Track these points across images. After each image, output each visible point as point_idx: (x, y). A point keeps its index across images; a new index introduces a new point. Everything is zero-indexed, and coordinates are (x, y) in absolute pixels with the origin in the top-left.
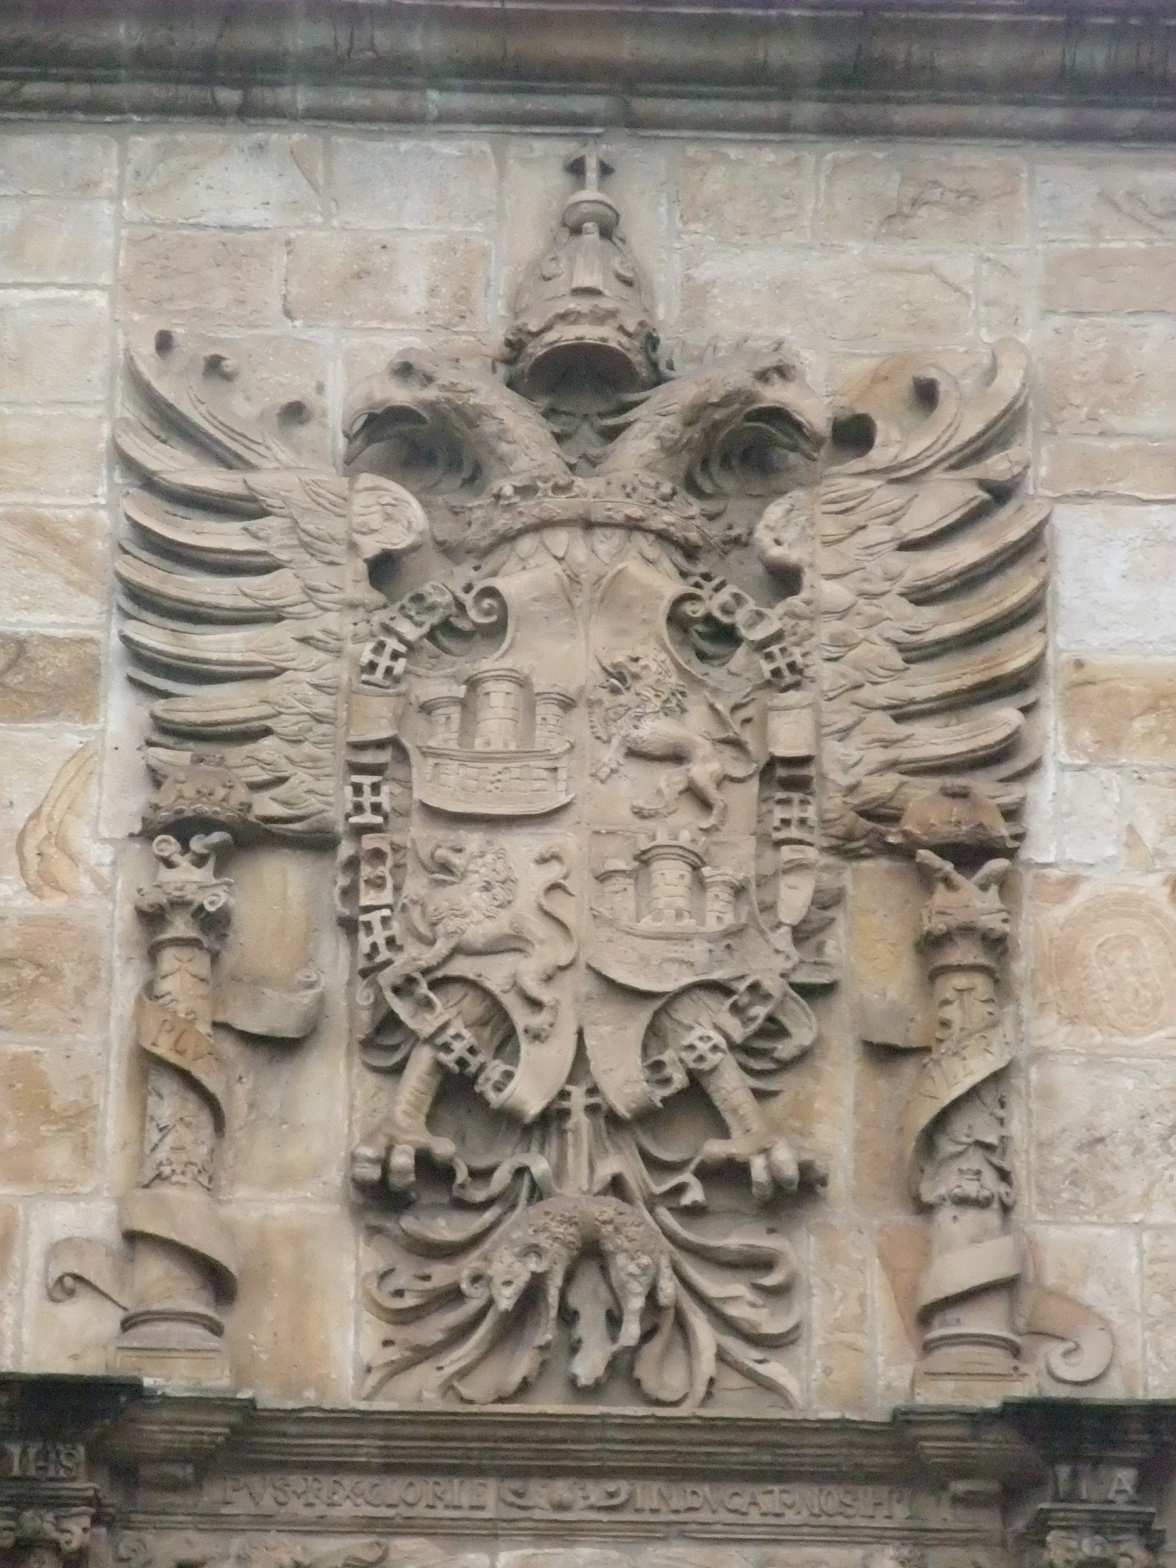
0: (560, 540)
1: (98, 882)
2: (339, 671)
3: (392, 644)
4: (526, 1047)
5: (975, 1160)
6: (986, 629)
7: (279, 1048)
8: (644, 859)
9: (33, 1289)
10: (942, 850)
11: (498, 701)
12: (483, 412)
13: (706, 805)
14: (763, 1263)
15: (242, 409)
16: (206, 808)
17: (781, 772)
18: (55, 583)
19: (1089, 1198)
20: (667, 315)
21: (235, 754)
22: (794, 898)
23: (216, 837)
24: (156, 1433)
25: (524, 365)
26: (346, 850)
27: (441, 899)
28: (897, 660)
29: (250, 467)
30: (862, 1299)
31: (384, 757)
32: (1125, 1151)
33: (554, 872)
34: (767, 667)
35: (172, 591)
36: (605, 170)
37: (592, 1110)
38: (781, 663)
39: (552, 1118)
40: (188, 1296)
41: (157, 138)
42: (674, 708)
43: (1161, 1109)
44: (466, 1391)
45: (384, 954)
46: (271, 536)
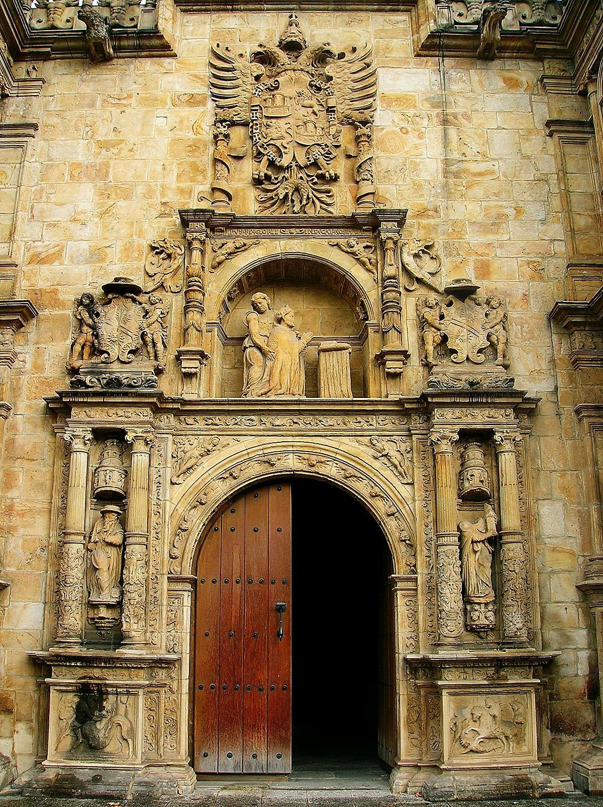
5: (367, 173)
6: (366, 87)
7: (238, 158)
11: (279, 98)
22: (333, 130)
24: (218, 221)
27: (268, 131)
33: (288, 126)
39: (289, 167)
40: (224, 197)
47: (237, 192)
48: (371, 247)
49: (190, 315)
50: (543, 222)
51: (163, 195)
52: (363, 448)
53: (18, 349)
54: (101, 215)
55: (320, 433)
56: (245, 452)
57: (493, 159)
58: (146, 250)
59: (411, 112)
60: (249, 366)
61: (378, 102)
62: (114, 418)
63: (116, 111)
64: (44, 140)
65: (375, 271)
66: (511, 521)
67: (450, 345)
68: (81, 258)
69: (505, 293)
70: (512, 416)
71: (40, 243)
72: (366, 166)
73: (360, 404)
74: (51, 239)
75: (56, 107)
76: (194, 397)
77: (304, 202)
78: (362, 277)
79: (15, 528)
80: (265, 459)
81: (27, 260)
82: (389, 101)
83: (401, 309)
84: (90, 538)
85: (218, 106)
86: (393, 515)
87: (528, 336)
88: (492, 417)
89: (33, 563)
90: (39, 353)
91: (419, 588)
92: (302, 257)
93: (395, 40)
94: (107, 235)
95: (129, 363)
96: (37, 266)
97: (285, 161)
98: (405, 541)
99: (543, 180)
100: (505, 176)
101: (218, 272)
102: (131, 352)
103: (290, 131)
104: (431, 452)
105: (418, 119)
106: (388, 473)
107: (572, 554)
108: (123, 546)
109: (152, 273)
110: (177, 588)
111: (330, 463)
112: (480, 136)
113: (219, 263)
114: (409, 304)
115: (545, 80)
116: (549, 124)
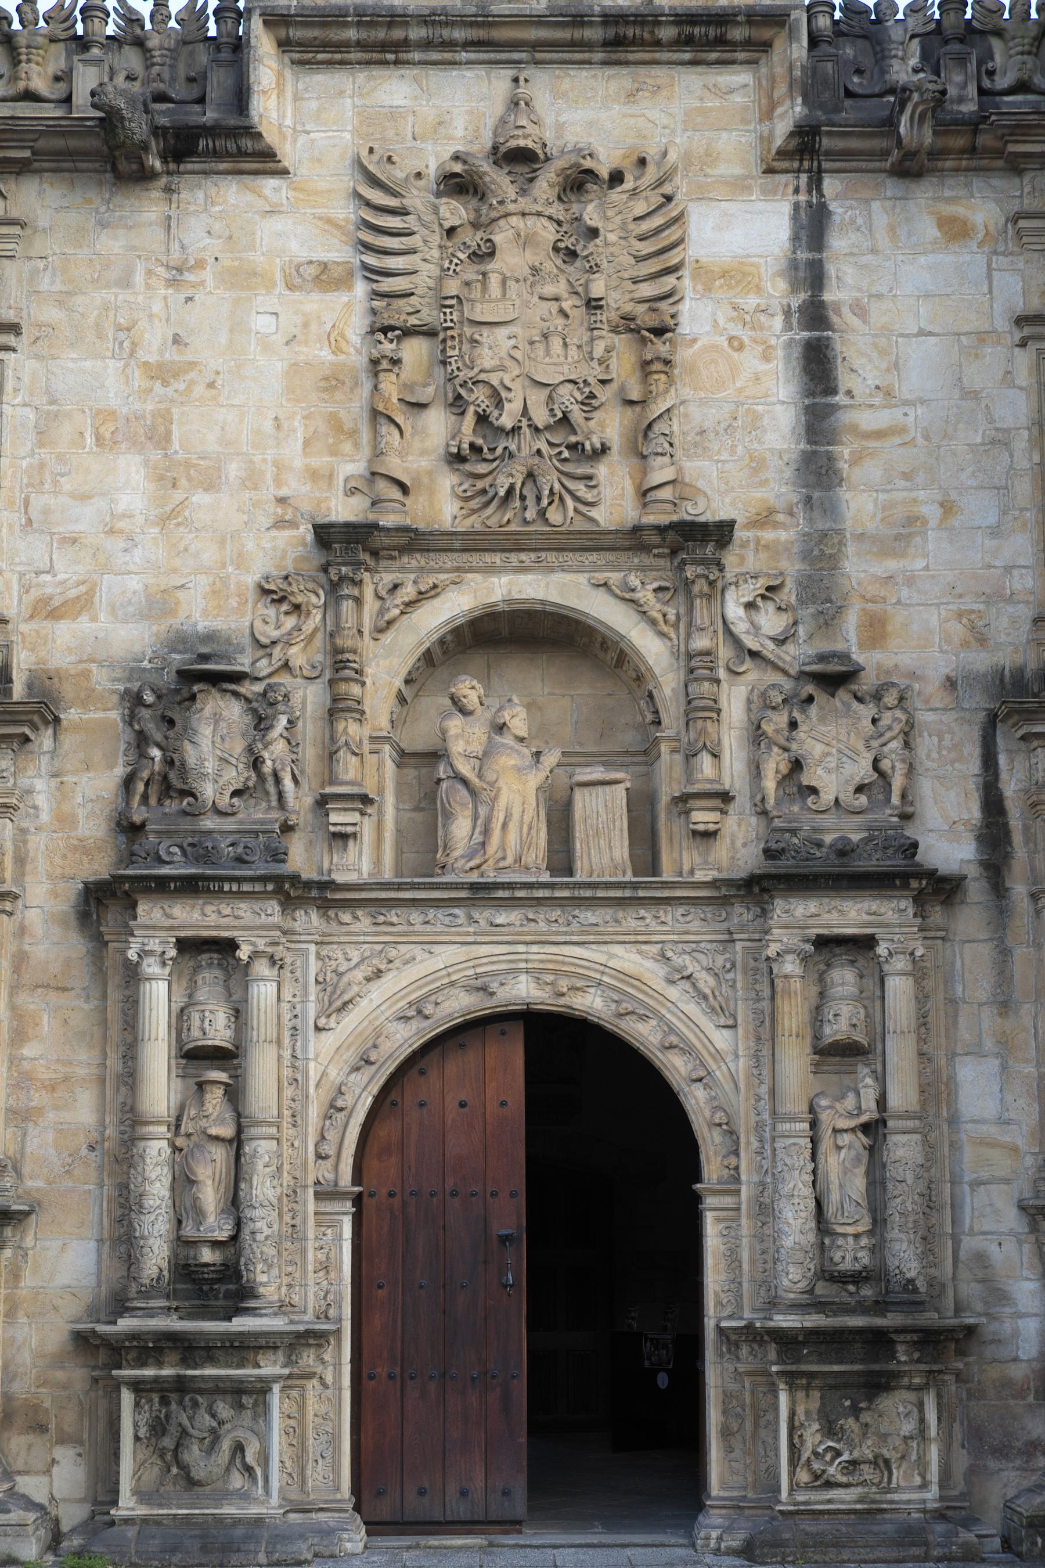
0: (514, 220)
1: (357, 350)
2: (435, 271)
3: (455, 261)
4: (507, 405)
5: (662, 439)
8: (545, 336)
9: (341, 493)
10: (649, 330)
11: (494, 280)
12: (485, 173)
13: (567, 316)
14: (590, 478)
15: (398, 173)
16: (392, 322)
17: (593, 303)
18: (337, 241)
19: (700, 451)
20: (549, 135)
21: (401, 302)
22: (599, 350)
23: (398, 332)
25: (500, 155)
26: (441, 336)
28: (633, 261)
29: (403, 197)
31: (454, 302)
32: (712, 435)
33: (513, 342)
34: (588, 266)
35: (377, 243)
36: (526, 81)
37: (529, 426)
38: (593, 263)
39: (515, 430)
40: (396, 494)
42: (555, 279)
44: (489, 523)
45: (456, 373)
47: (417, 479)
48: (667, 589)
49: (340, 726)
50: (995, 532)
51: (278, 482)
52: (649, 964)
53: (24, 782)
54: (163, 521)
55: (575, 938)
56: (444, 972)
57: (906, 403)
58: (251, 595)
59: (751, 302)
60: (448, 816)
61: (687, 282)
62: (213, 919)
64: (38, 357)
65: (673, 636)
66: (902, 1095)
67: (806, 779)
68: (131, 609)
69: (913, 675)
70: (911, 911)
71: (48, 578)
72: (659, 427)
73: (643, 887)
74: (69, 572)
75: (53, 283)
76: (352, 878)
77: (545, 502)
78: (651, 648)
79: (40, 1110)
80: (479, 983)
81: (26, 612)
83: (719, 711)
84: (178, 1126)
85: (377, 295)
86: (700, 1080)
87: (953, 755)
88: (875, 914)
89: (76, 1172)
90: (62, 792)
91: (744, 1207)
92: (539, 607)
93: (724, 135)
94: (177, 562)
95: (233, 814)
96: (47, 624)
97: (507, 421)
98: (720, 1125)
99: (1000, 441)
100: (927, 438)
101: (388, 638)
102: (236, 793)
103: (518, 354)
104: (764, 971)
105: (763, 318)
106: (692, 1009)
107: (1014, 1149)
108: (237, 1143)
109: (264, 640)
110: (328, 1210)
111: (592, 990)
112: (883, 352)
113: (390, 623)
114: (734, 701)
115: (1022, 223)
116: (1021, 321)
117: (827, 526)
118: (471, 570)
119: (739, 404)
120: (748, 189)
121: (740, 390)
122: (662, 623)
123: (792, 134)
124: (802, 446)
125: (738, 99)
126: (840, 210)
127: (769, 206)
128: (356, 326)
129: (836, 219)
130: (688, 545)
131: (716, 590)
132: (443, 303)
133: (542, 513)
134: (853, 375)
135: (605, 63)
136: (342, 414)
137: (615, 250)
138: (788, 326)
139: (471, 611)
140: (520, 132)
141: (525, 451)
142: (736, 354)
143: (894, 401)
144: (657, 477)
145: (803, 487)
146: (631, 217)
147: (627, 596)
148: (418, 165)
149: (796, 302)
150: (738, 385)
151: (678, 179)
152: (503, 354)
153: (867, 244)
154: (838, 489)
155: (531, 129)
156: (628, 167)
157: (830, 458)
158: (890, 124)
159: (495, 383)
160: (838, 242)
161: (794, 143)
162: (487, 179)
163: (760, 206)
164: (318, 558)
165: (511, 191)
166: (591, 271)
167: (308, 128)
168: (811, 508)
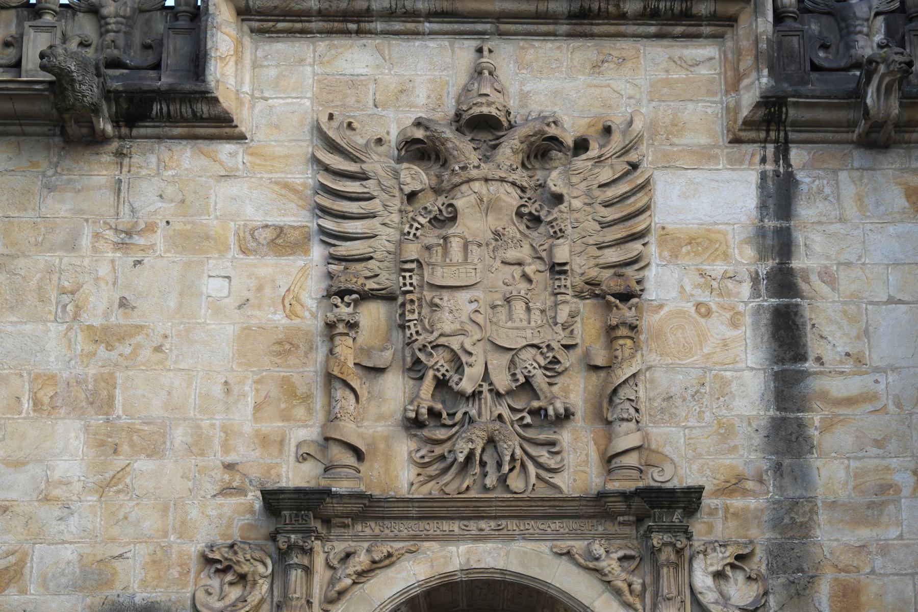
0: (476, 186)
1: (312, 314)
2: (395, 235)
3: (416, 225)
5: (627, 405)
7: (379, 371)
8: (508, 300)
9: (292, 458)
10: (614, 295)
11: (456, 245)
12: (447, 139)
13: (530, 281)
14: (553, 444)
16: (349, 286)
17: (557, 268)
18: (294, 206)
19: (666, 417)
20: (512, 104)
21: (359, 266)
22: (563, 314)
23: (355, 296)
25: (462, 122)
26: (400, 300)
28: (598, 227)
29: (363, 162)
30: (587, 455)
31: (414, 266)
32: (679, 401)
33: (474, 306)
34: (551, 231)
35: (335, 207)
36: (490, 51)
37: (490, 391)
38: (557, 229)
39: (476, 395)
41: (327, 43)
42: (519, 244)
43: (693, 386)
44: (447, 490)
45: (415, 337)
46: (371, 186)
57: (877, 370)
59: (718, 268)
61: (653, 248)
63: (125, 261)
65: (639, 606)
72: (624, 393)
77: (506, 468)
82: (678, 244)
92: (498, 577)
93: (690, 106)
97: (467, 386)
100: (899, 405)
103: (479, 319)
105: (730, 284)
112: (853, 320)
117: (798, 493)
118: (428, 538)
119: (706, 370)
120: (715, 158)
121: (708, 356)
122: (627, 593)
123: (758, 105)
124: (771, 413)
125: (704, 71)
126: (807, 180)
127: (735, 175)
128: (311, 290)
129: (804, 188)
130: (655, 513)
131: (683, 559)
132: (402, 267)
133: (503, 480)
134: (822, 342)
135: (570, 35)
136: (296, 378)
137: (580, 215)
138: (756, 293)
139: (427, 581)
140: (483, 100)
141: (486, 416)
142: (703, 321)
143: (864, 368)
144: (622, 444)
145: (773, 454)
146: (596, 183)
147: (591, 565)
148: (380, 132)
149: (764, 269)
150: (706, 350)
151: (643, 148)
152: (464, 318)
153: (835, 213)
154: (809, 456)
155: (494, 97)
156: (592, 134)
157: (801, 425)
158: (858, 94)
159: (456, 347)
160: (806, 211)
161: (761, 113)
162: (450, 145)
163: (727, 174)
164: (266, 526)
165: (474, 158)
166: (555, 236)
167: (266, 95)
168: (782, 475)
